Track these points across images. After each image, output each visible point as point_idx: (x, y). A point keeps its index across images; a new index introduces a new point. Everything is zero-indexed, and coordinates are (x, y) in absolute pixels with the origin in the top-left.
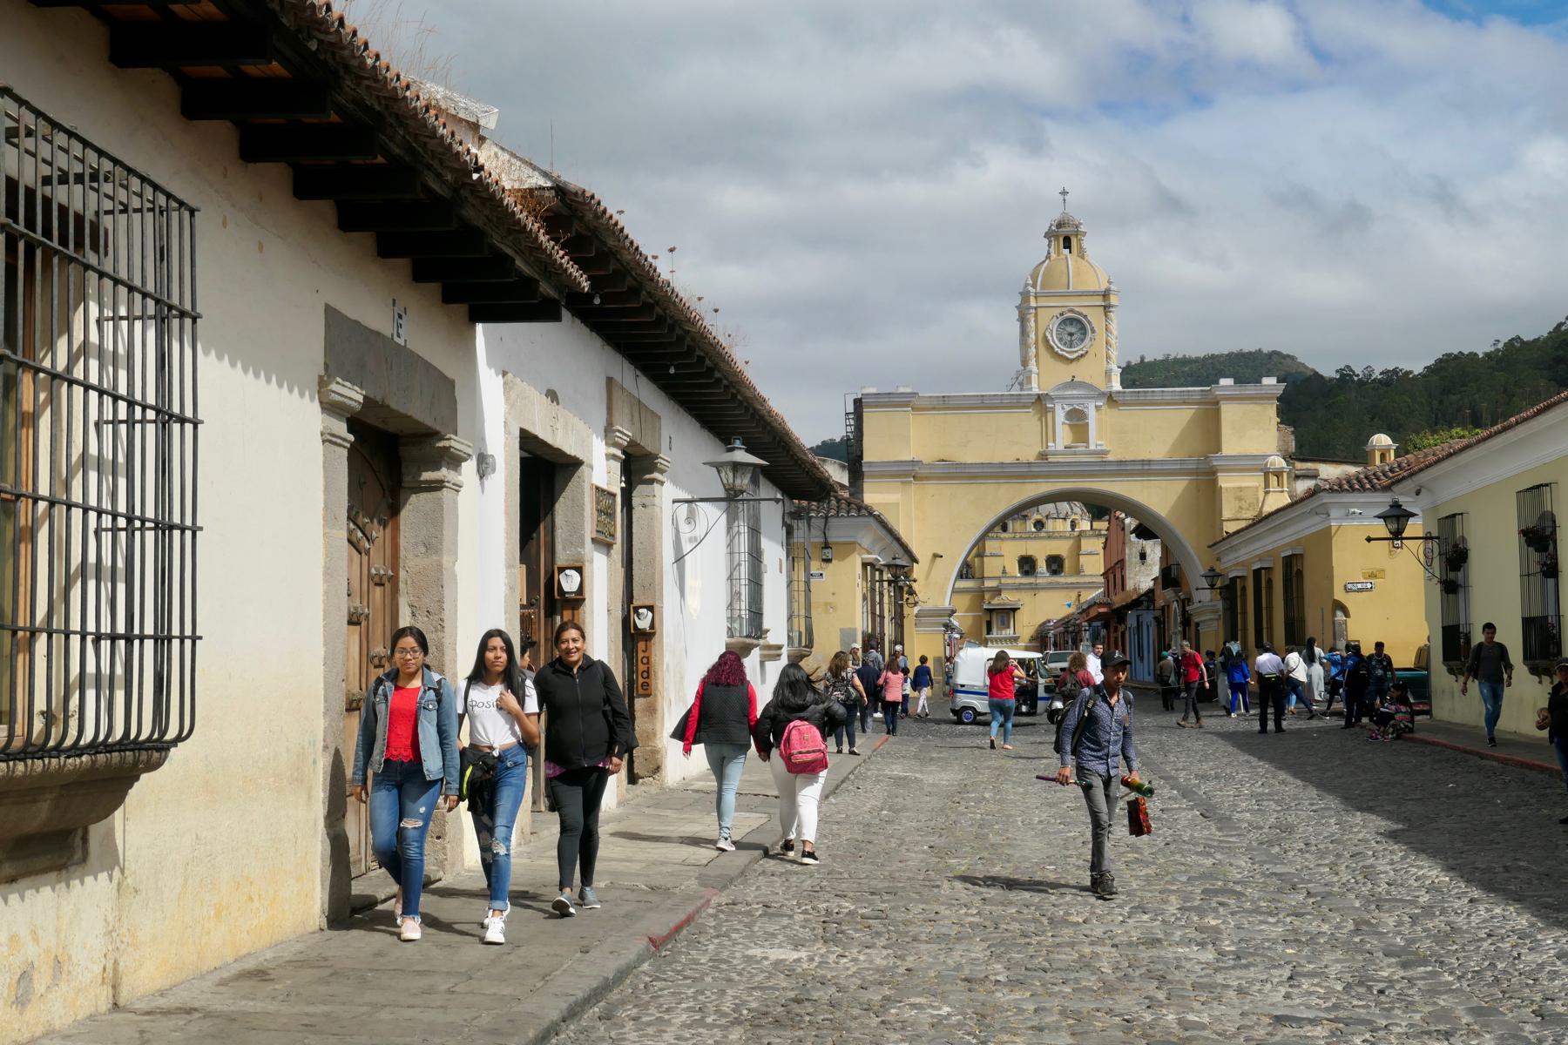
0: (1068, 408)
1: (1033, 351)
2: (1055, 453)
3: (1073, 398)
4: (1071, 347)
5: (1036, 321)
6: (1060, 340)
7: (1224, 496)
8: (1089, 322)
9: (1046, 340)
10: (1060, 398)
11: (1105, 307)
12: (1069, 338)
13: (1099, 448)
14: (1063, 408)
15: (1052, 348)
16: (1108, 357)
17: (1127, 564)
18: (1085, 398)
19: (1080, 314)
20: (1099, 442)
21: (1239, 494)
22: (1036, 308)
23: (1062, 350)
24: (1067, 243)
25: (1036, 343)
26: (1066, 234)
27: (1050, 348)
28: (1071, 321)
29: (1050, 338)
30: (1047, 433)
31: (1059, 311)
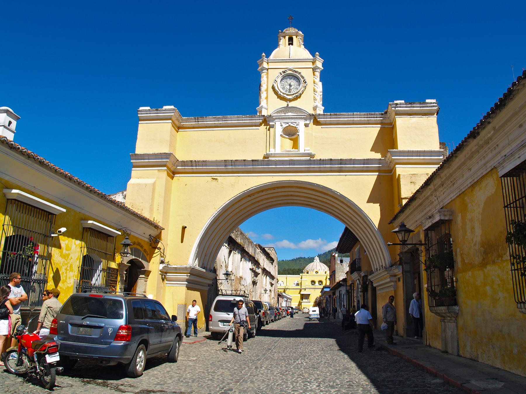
0: (285, 126)
1: (263, 95)
2: (275, 155)
3: (289, 118)
5: (267, 77)
6: (283, 88)
7: (402, 182)
8: (303, 77)
9: (273, 88)
10: (279, 118)
13: (306, 152)
14: (282, 126)
16: (315, 99)
17: (336, 272)
18: (296, 118)
19: (296, 72)
20: (306, 149)
21: (413, 179)
22: (267, 69)
23: (283, 93)
25: (267, 90)
26: (290, 34)
27: (276, 93)
30: (270, 142)
31: (281, 71)
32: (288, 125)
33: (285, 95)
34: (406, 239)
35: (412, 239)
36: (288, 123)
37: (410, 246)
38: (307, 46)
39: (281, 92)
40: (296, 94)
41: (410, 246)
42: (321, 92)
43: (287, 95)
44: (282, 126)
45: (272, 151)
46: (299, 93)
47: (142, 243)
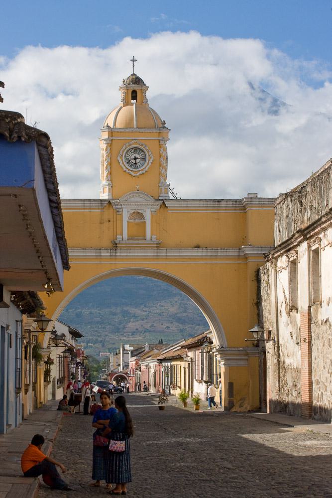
6: (128, 163)
11: (159, 141)
12: (134, 161)
23: (129, 170)
24: (134, 95)
28: (137, 150)
32: (134, 211)
39: (126, 168)
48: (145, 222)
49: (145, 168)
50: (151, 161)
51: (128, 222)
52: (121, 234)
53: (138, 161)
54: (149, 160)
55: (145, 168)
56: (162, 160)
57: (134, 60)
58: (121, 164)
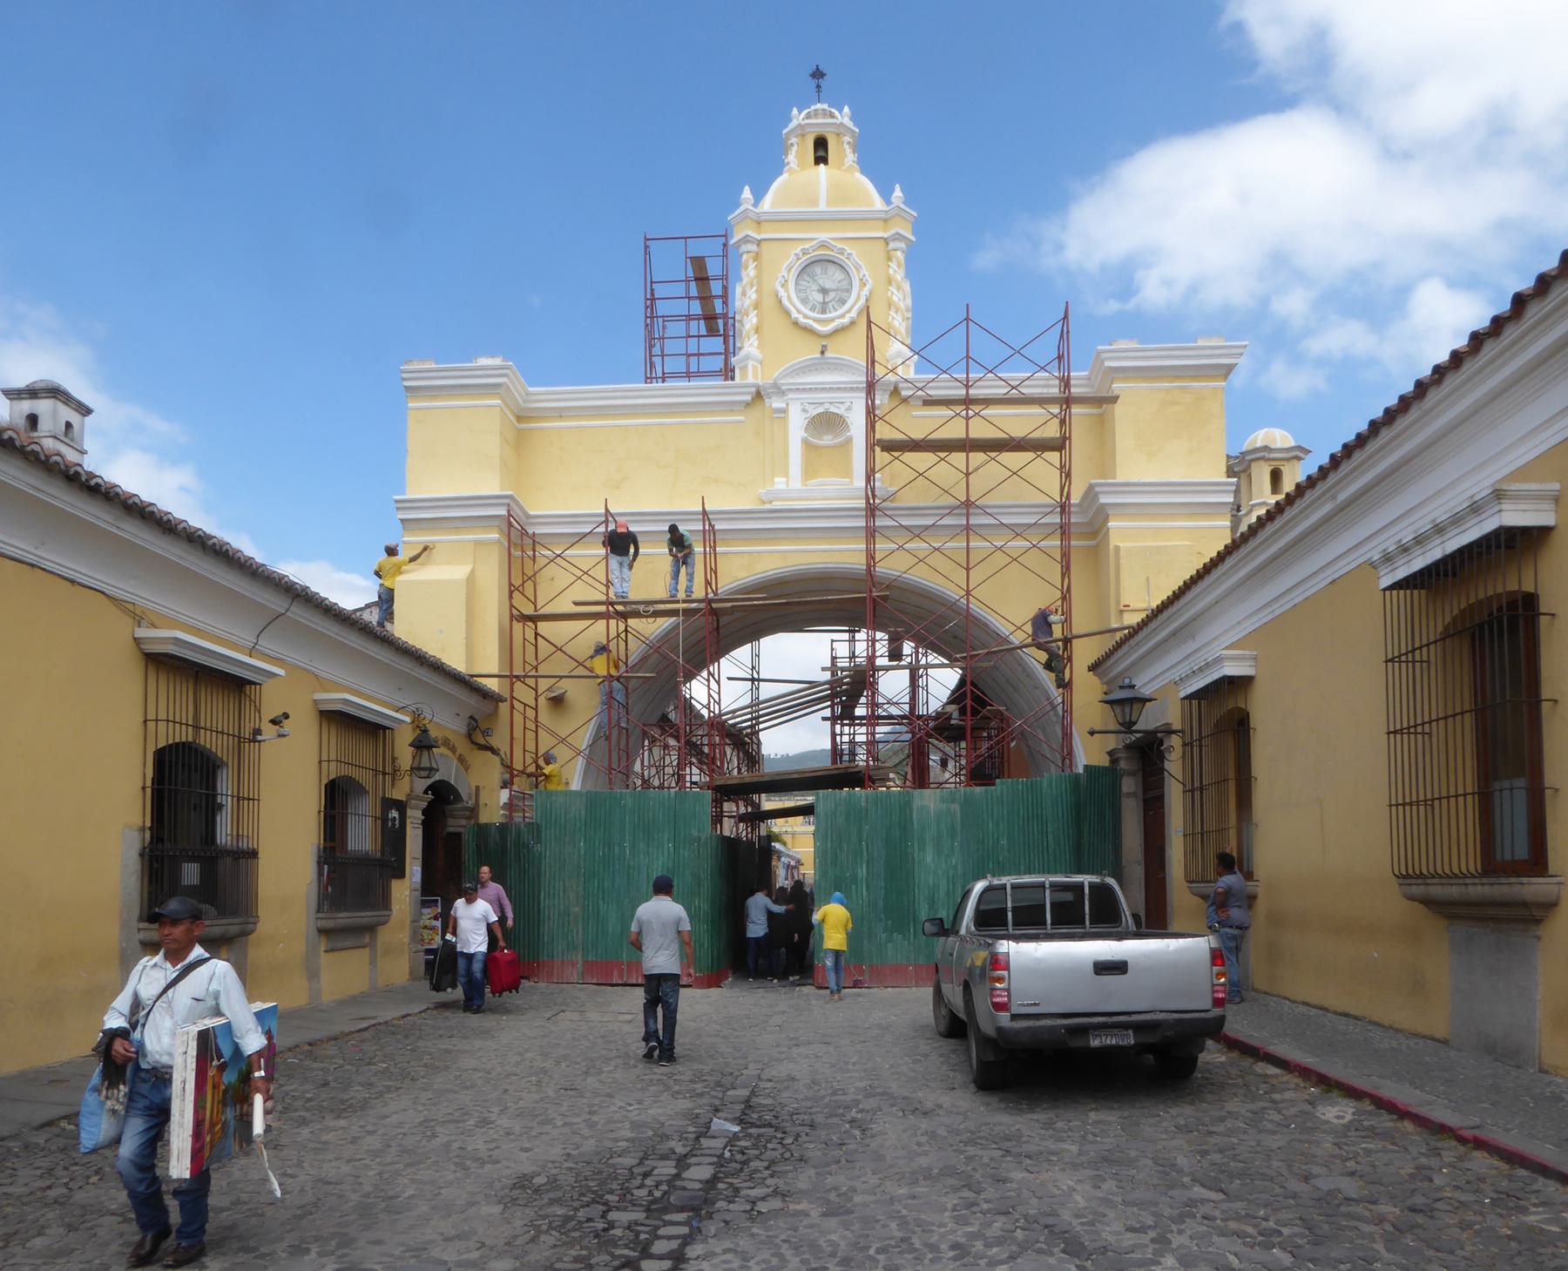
0: (814, 411)
4: (824, 311)
6: (804, 301)
12: (819, 297)
15: (787, 313)
19: (842, 251)
23: (806, 317)
29: (782, 293)
32: (821, 410)
33: (810, 322)
34: (1134, 719)
35: (1148, 720)
36: (822, 403)
37: (1138, 735)
38: (866, 167)
39: (799, 311)
40: (839, 317)
41: (1138, 735)
42: (907, 311)
43: (815, 320)
44: (804, 410)
45: (780, 483)
46: (848, 316)
47: (452, 738)
48: (849, 441)
49: (849, 311)
50: (866, 291)
51: (805, 442)
52: (786, 475)
53: (832, 295)
54: (860, 290)
55: (849, 311)
56: (895, 291)
57: (818, 74)
58: (785, 302)
